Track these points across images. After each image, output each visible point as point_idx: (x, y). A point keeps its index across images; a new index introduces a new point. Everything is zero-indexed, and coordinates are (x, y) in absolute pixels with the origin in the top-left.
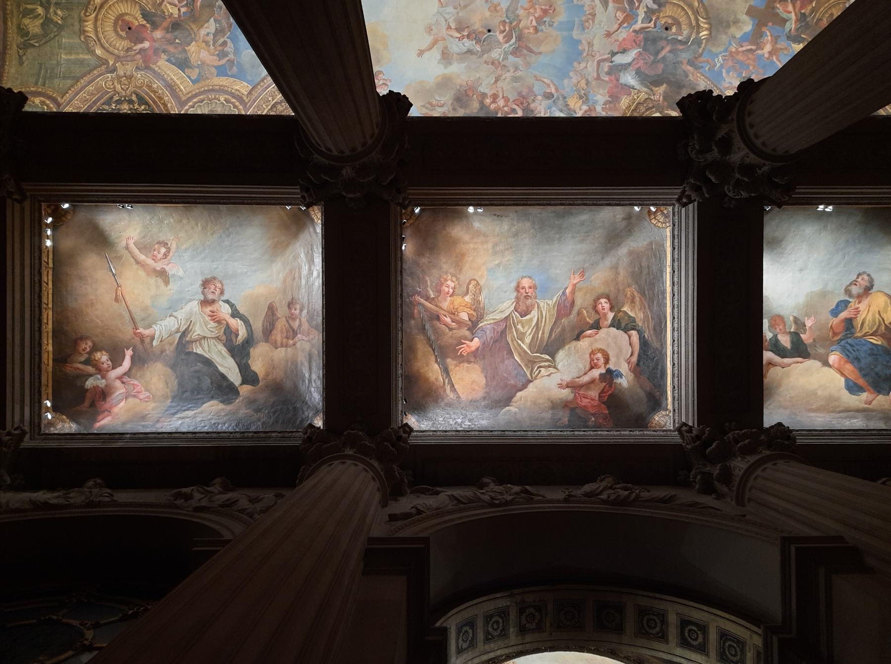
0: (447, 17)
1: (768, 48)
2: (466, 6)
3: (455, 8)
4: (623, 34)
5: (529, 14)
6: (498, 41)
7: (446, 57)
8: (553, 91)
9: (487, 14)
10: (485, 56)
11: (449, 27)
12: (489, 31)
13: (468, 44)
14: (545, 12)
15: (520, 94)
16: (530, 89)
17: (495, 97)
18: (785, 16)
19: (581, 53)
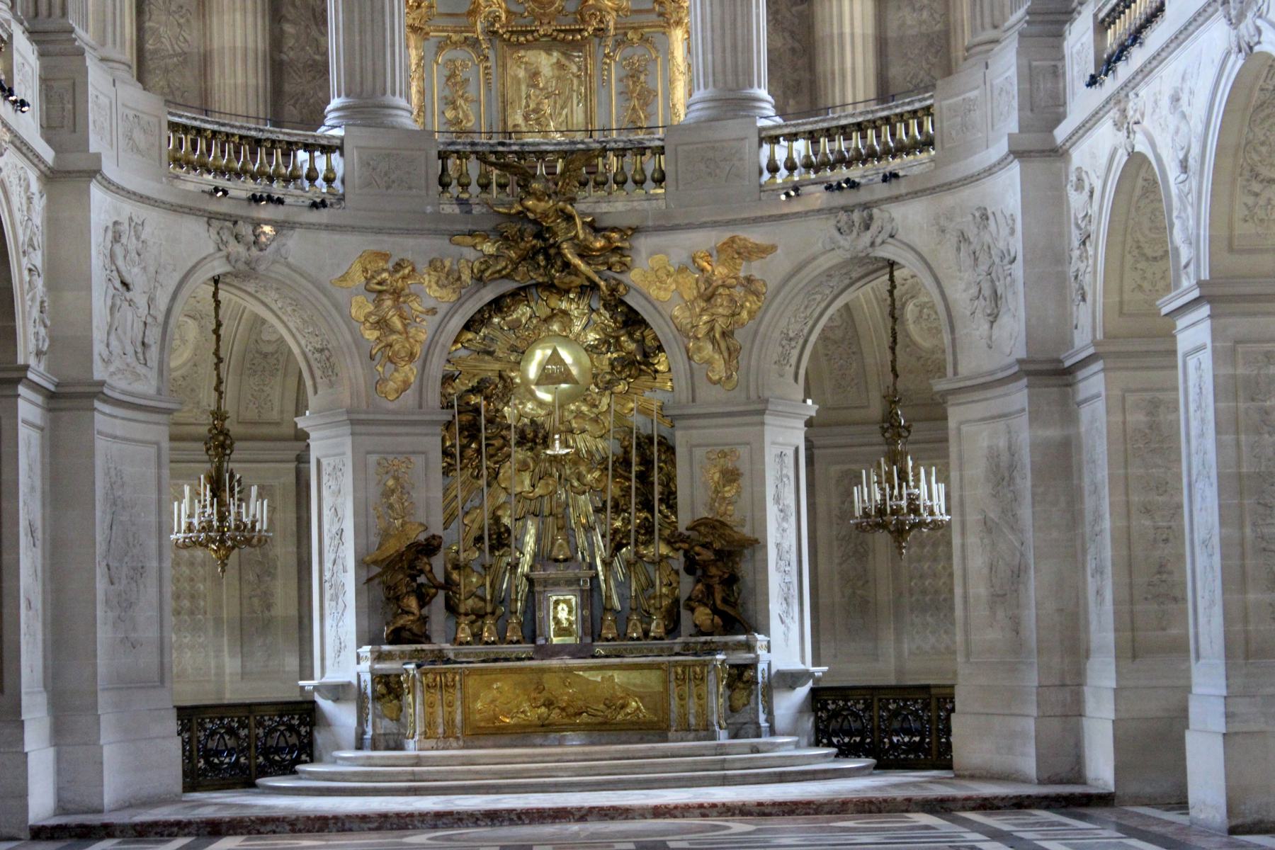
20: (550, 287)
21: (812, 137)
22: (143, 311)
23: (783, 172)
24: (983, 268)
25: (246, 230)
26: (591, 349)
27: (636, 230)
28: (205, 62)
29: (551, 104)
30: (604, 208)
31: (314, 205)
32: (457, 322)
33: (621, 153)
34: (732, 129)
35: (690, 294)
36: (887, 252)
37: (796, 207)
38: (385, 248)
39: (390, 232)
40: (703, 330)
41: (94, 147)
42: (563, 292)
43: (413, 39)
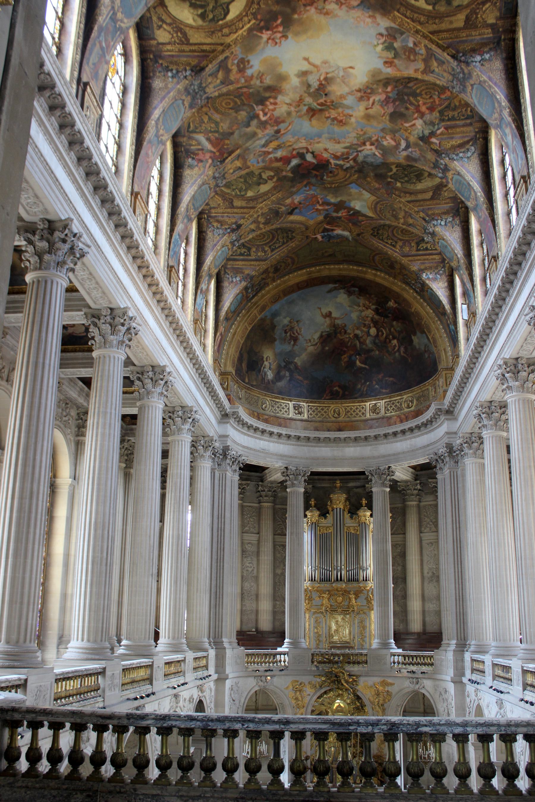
0: (336, 72)
1: (320, 208)
2: (344, 82)
3: (343, 76)
4: (325, 155)
5: (339, 114)
6: (318, 100)
7: (304, 74)
8: (282, 132)
9: (339, 93)
10: (306, 95)
11: (327, 73)
12: (326, 95)
13: (315, 85)
14: (341, 121)
15: (279, 118)
16: (283, 122)
17: (275, 104)
18: (341, 212)
19: (311, 139)
20: (338, 688)
21: (404, 656)
22: (237, 705)
23: (396, 665)
24: (445, 704)
25: (263, 678)
26: (348, 704)
27: (360, 676)
28: (257, 611)
29: (341, 629)
30: (352, 669)
31: (281, 670)
32: (315, 697)
33: (357, 655)
34: (384, 652)
35: (373, 693)
36: (423, 691)
37: (400, 675)
38: (297, 679)
39: (299, 675)
40: (376, 703)
41: (227, 672)
42: (341, 690)
43: (307, 612)
